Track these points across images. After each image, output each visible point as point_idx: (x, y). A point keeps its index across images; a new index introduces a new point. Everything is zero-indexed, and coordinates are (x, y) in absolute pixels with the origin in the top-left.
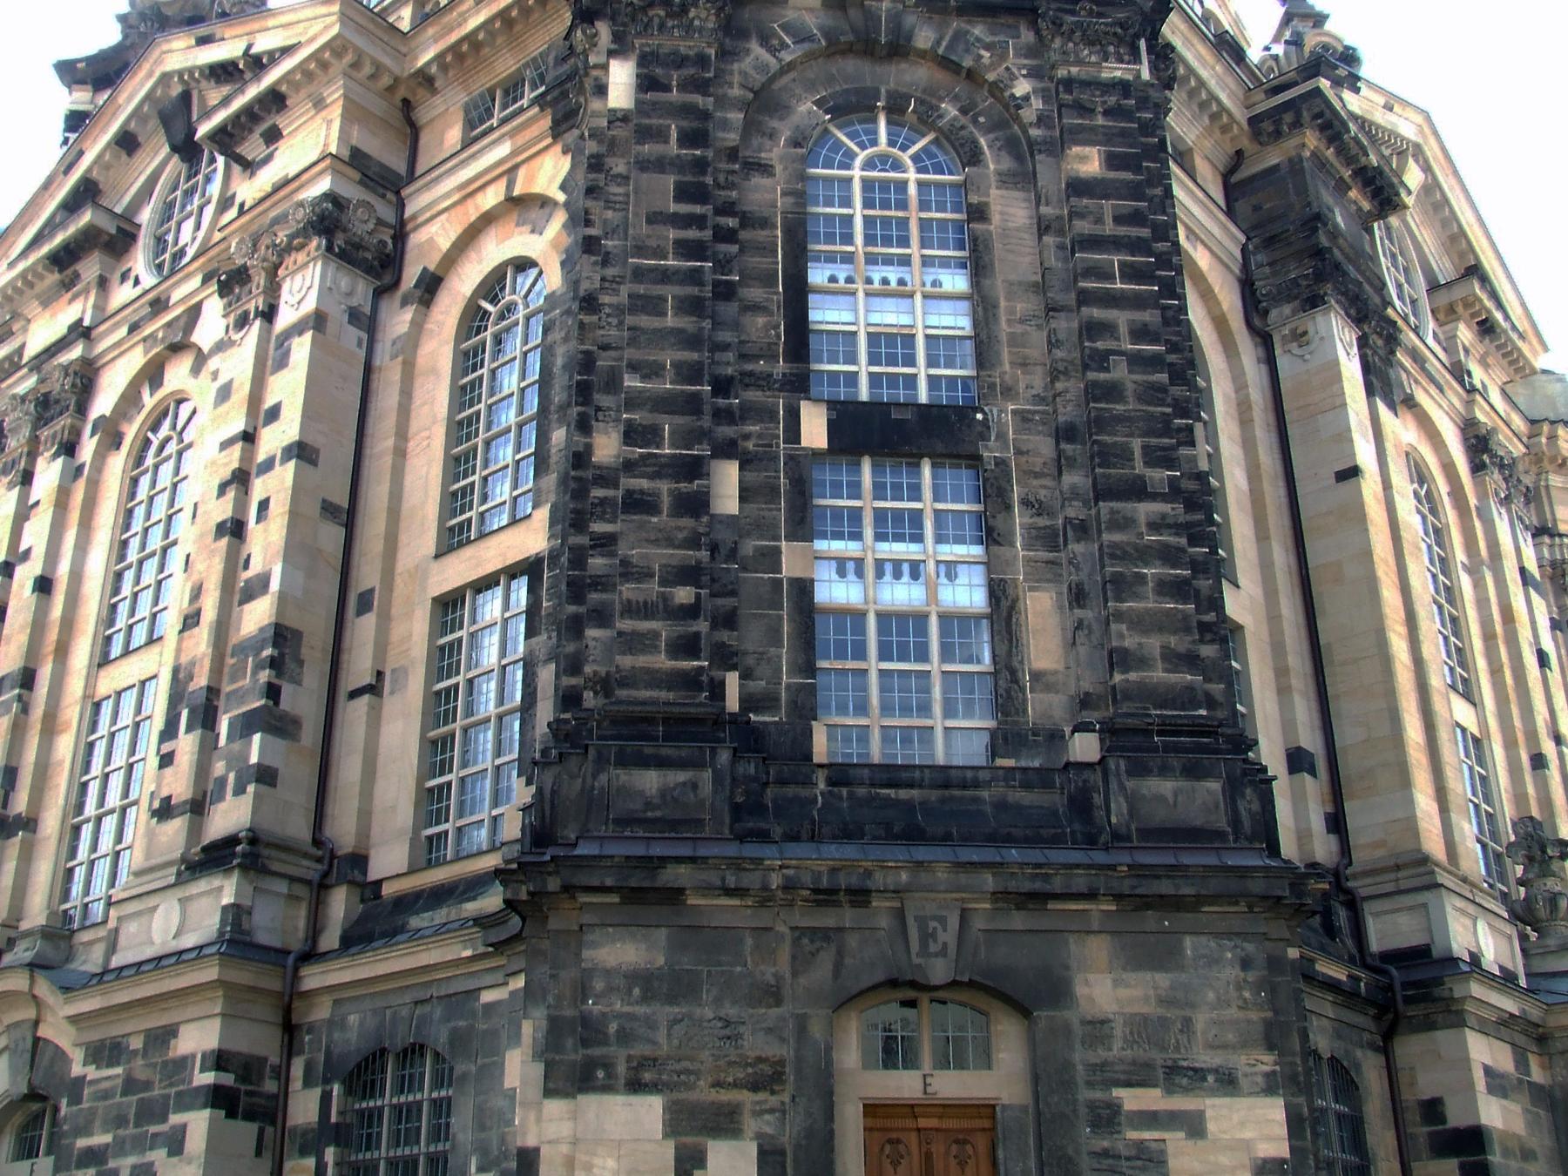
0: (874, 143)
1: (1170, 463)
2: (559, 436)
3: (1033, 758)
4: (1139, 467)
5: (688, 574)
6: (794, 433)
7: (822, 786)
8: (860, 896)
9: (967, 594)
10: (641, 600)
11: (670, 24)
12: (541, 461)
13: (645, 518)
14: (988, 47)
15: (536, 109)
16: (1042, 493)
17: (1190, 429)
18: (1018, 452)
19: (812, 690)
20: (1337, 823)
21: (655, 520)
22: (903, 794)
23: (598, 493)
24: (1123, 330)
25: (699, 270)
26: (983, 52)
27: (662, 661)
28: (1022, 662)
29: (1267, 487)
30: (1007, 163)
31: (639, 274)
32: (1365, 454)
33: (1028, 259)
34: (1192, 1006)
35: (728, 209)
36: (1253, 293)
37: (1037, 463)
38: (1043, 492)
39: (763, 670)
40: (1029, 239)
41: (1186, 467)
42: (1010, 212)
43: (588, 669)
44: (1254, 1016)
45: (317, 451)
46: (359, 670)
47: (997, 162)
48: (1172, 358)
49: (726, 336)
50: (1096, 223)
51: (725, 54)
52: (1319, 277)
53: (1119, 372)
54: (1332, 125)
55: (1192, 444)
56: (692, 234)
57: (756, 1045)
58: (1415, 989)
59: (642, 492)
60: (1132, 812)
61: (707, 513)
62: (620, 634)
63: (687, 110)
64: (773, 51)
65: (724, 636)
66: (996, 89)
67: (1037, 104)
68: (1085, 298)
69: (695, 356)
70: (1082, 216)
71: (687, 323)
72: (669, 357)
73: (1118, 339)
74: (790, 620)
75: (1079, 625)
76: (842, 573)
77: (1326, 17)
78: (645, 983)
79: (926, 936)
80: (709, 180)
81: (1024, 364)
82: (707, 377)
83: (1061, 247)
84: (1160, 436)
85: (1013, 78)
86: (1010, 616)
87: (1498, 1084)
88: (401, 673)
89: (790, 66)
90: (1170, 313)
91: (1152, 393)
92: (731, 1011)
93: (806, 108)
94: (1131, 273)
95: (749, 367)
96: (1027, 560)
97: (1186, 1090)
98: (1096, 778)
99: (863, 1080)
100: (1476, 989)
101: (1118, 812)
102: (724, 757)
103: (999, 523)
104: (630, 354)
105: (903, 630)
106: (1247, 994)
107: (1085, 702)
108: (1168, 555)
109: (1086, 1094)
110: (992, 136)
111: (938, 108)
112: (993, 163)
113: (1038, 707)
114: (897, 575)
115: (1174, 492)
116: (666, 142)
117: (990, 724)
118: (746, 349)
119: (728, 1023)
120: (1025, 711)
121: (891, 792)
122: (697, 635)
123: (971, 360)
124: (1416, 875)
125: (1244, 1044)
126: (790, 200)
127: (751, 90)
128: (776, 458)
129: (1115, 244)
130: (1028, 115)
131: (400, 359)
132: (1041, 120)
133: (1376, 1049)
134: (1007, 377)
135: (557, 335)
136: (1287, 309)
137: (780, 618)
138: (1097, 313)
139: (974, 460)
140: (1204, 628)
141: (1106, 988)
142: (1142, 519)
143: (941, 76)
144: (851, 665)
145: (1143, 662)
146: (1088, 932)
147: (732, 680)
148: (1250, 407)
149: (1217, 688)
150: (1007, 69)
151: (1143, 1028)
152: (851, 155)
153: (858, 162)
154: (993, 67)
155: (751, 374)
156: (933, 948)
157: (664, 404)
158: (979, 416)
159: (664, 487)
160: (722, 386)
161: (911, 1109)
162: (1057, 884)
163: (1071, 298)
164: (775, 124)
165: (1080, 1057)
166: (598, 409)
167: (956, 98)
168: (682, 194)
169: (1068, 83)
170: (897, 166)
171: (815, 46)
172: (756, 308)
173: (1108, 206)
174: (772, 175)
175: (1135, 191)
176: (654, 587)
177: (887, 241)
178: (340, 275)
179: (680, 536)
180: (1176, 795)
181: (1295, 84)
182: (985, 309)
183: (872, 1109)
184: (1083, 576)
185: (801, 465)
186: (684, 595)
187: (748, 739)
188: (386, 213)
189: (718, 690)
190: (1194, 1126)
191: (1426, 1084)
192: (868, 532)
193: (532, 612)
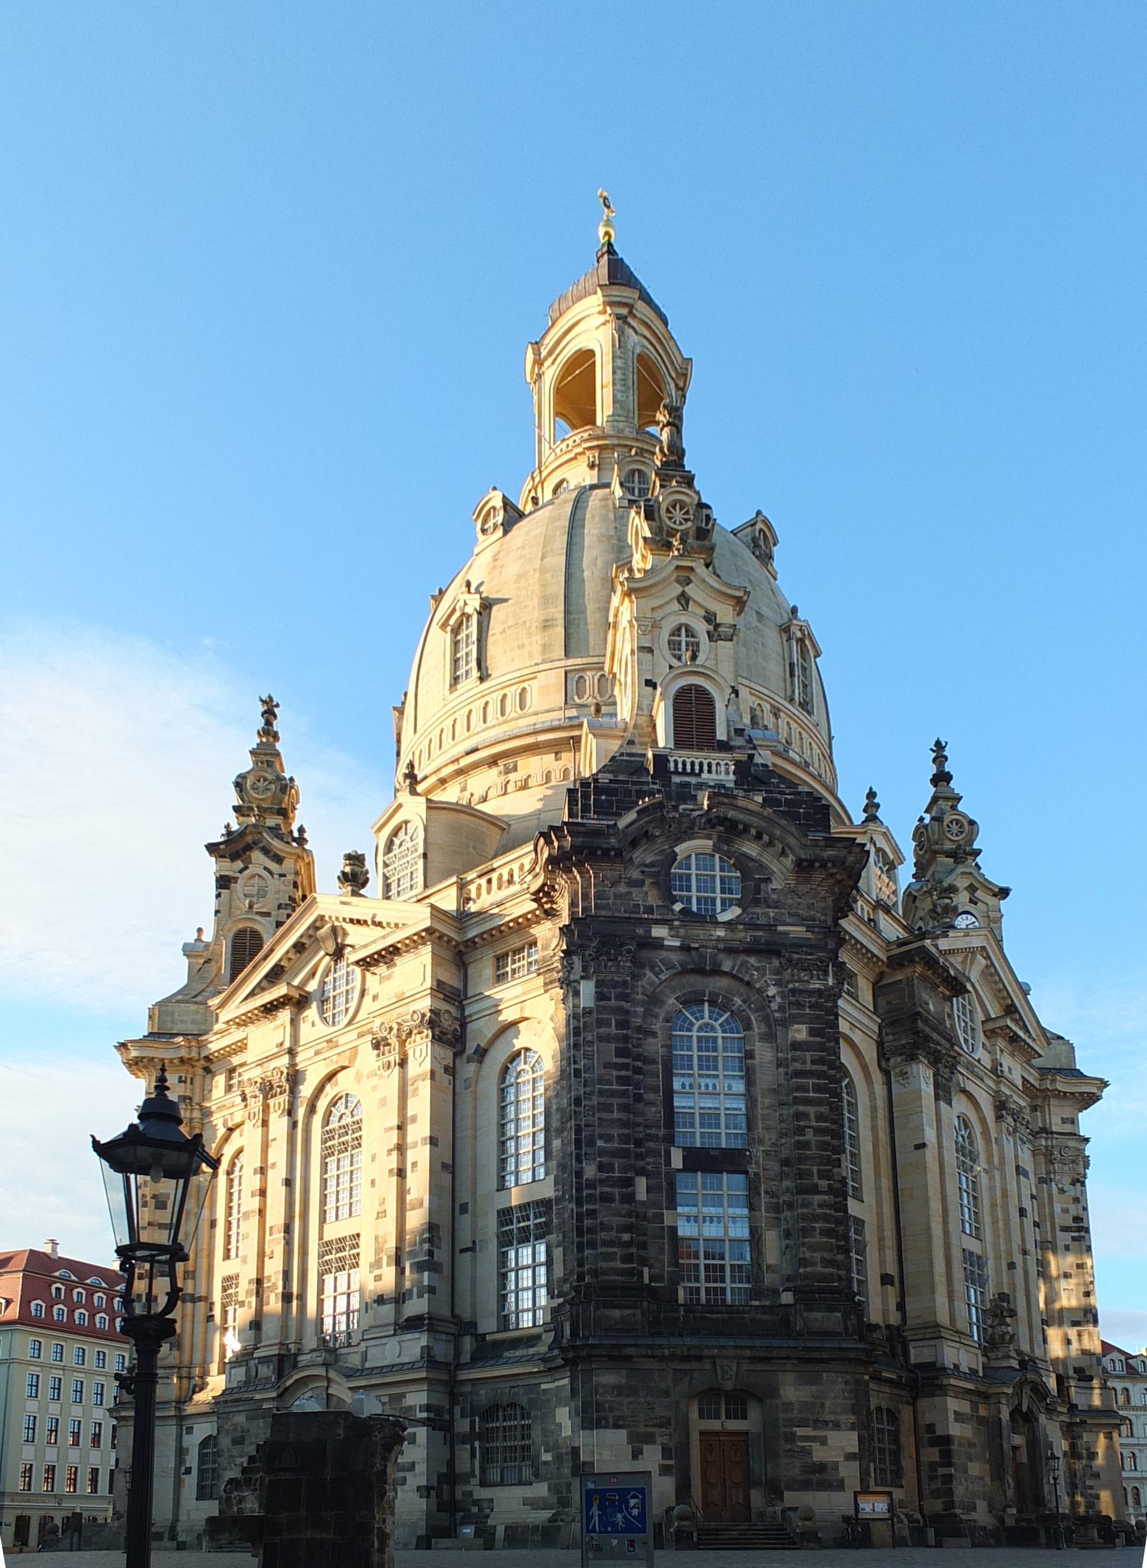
0: (702, 1017)
2: (556, 1143)
4: (816, 1180)
8: (699, 1358)
9: (741, 1231)
16: (774, 1189)
17: (839, 1160)
18: (764, 1169)
22: (714, 1316)
23: (590, 1192)
24: (812, 1116)
27: (619, 1265)
30: (764, 1029)
31: (601, 1093)
33: (770, 1078)
35: (638, 1058)
40: (773, 1067)
41: (836, 1178)
42: (764, 1053)
49: (639, 1120)
51: (635, 977)
52: (915, 1046)
53: (810, 1135)
55: (840, 1166)
56: (623, 1073)
57: (660, 1412)
58: (928, 1380)
61: (635, 1201)
63: (619, 1010)
64: (656, 974)
65: (642, 1252)
67: (778, 999)
69: (627, 1131)
71: (623, 1116)
75: (787, 1247)
79: (724, 1372)
80: (630, 1046)
83: (786, 1074)
85: (768, 986)
87: (960, 1417)
89: (665, 981)
91: (823, 1146)
94: (817, 1089)
99: (698, 1425)
101: (799, 1325)
102: (645, 1304)
107: (789, 1278)
108: (825, 1218)
109: (783, 1429)
112: (757, 1028)
113: (770, 1279)
114: (711, 1222)
115: (830, 1190)
123: (744, 1125)
126: (665, 1049)
128: (660, 1173)
130: (774, 1006)
132: (781, 1008)
136: (899, 1059)
138: (801, 1108)
139: (746, 1172)
141: (792, 1391)
142: (816, 1203)
143: (734, 983)
144: (693, 1261)
145: (813, 1264)
147: (646, 1270)
149: (843, 1273)
152: (692, 1024)
153: (695, 1028)
154: (759, 980)
155: (649, 1135)
157: (615, 1154)
159: (616, 1190)
160: (638, 1143)
161: (716, 1433)
162: (775, 1354)
164: (657, 1010)
165: (781, 1416)
167: (741, 995)
170: (713, 1029)
172: (652, 1103)
173: (808, 1054)
175: (821, 1047)
177: (708, 1069)
186: (626, 1237)
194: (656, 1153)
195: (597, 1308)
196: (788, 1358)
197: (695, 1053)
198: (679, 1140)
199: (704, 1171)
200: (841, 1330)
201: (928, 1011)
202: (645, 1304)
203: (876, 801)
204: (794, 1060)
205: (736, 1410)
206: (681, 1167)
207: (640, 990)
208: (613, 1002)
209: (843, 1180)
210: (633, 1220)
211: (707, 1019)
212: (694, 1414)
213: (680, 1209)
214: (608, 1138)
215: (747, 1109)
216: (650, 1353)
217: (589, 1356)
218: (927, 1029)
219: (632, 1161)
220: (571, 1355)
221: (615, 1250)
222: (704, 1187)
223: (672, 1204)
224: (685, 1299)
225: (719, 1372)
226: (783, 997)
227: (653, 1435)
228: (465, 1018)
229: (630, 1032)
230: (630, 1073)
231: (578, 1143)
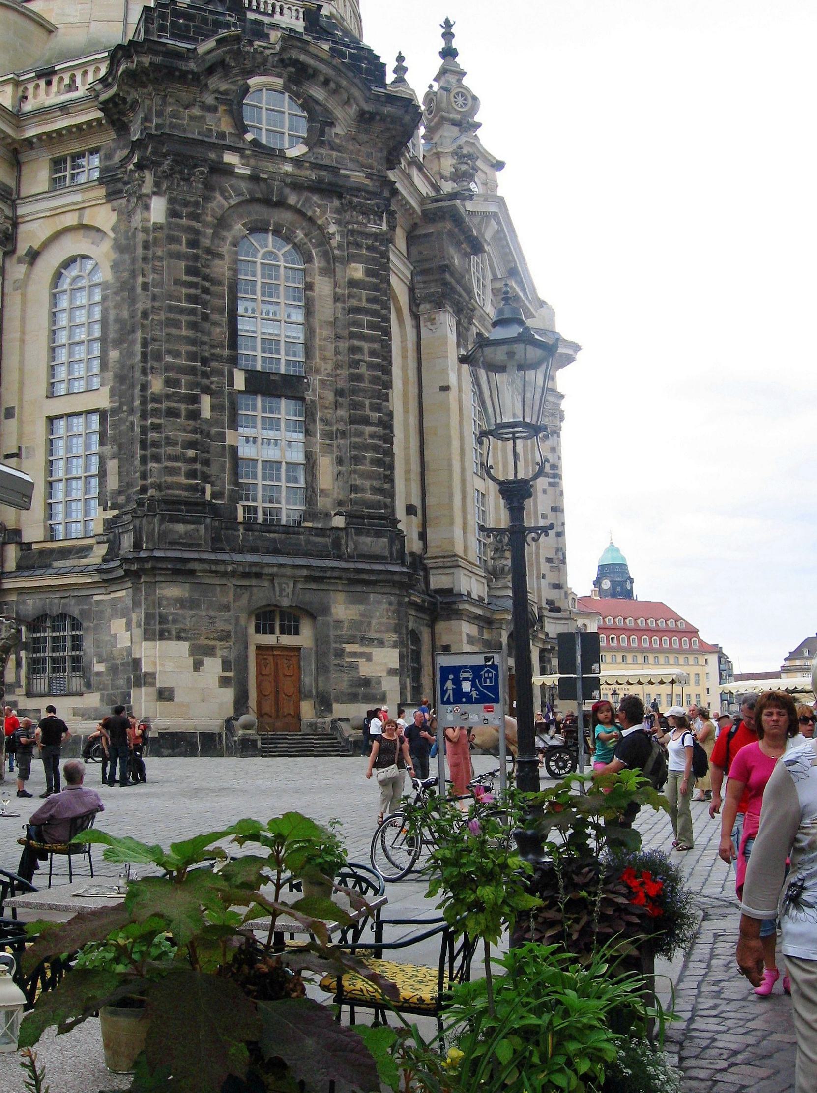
2: (114, 355)
4: (368, 412)
6: (231, 383)
7: (242, 530)
8: (258, 575)
9: (297, 456)
11: (182, 183)
12: (104, 366)
14: (319, 206)
15: (97, 183)
17: (387, 394)
18: (320, 398)
20: (423, 536)
22: (272, 535)
23: (156, 406)
24: (366, 351)
27: (183, 480)
30: (323, 264)
31: (171, 309)
32: (453, 380)
34: (371, 617)
35: (206, 278)
36: (414, 294)
38: (329, 416)
39: (218, 482)
40: (330, 301)
41: (384, 411)
42: (323, 287)
44: (392, 622)
47: (319, 263)
48: (384, 363)
49: (206, 338)
51: (207, 199)
52: (444, 295)
53: (363, 369)
54: (457, 219)
56: (192, 291)
57: (220, 625)
58: (443, 606)
59: (174, 408)
60: (356, 548)
63: (190, 230)
64: (226, 198)
65: (205, 469)
66: (321, 228)
67: (338, 238)
68: (352, 335)
71: (190, 333)
74: (230, 463)
75: (339, 473)
76: (247, 441)
77: (464, 74)
78: (181, 602)
79: (282, 590)
80: (199, 265)
81: (324, 359)
82: (199, 359)
83: (344, 309)
85: (329, 223)
86: (313, 467)
90: (384, 343)
91: (375, 380)
92: (212, 614)
93: (238, 228)
94: (372, 326)
95: (213, 351)
96: (321, 444)
97: (367, 646)
98: (343, 534)
100: (467, 607)
101: (351, 546)
102: (208, 521)
103: (311, 427)
104: (170, 346)
105: (272, 466)
107: (340, 503)
108: (375, 448)
112: (318, 262)
113: (322, 503)
115: (381, 423)
116: (181, 245)
117: (303, 508)
118: (215, 343)
119: (211, 618)
124: (451, 562)
125: (388, 631)
126: (231, 273)
129: (367, 311)
130: (334, 243)
131: (19, 291)
132: (339, 247)
133: (428, 626)
135: (110, 304)
136: (428, 306)
138: (356, 342)
140: (386, 476)
141: (342, 609)
142: (367, 433)
145: (363, 490)
147: (208, 487)
148: (407, 351)
151: (354, 624)
153: (260, 255)
154: (320, 218)
156: (284, 594)
159: (183, 407)
160: (205, 361)
161: (271, 648)
162: (328, 574)
163: (345, 333)
164: (225, 234)
165: (332, 633)
166: (152, 368)
167: (303, 229)
168: (190, 271)
169: (352, 232)
172: (215, 324)
173: (364, 292)
175: (376, 288)
176: (179, 449)
179: (190, 428)
183: (259, 648)
184: (342, 453)
185: (233, 396)
186: (191, 453)
187: (215, 510)
188: (8, 212)
190: (369, 657)
191: (445, 640)
192: (259, 425)
193: (103, 435)
194: (221, 374)
195: (162, 521)
196: (340, 578)
197: (259, 280)
198: (242, 363)
199: (264, 394)
200: (387, 554)
201: (453, 265)
202: (208, 521)
203: (404, 64)
204: (350, 296)
205: (289, 627)
206: (244, 389)
208: (184, 221)
209: (390, 415)
210: (198, 436)
211: (270, 248)
212: (252, 630)
213: (241, 430)
214: (176, 354)
215: (306, 339)
216: (214, 568)
217: (154, 568)
218: (453, 281)
219: (199, 379)
220: (135, 567)
221: (179, 464)
222: (264, 411)
223: (234, 424)
224: (244, 517)
225: (277, 589)
226: (342, 237)
227: (213, 648)
229: (200, 252)
230: (199, 292)
231: (144, 355)
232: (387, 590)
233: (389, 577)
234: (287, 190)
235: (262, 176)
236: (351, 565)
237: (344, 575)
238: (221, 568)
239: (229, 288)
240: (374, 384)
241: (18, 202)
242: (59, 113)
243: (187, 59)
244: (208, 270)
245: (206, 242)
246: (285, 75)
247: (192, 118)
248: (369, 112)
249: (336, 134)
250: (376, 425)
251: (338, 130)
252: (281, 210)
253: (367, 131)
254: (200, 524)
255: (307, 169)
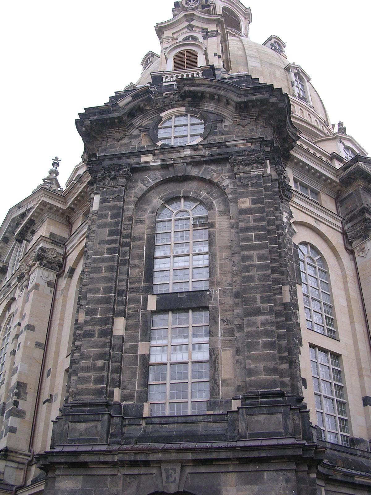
1: (269, 301)
3: (220, 410)
4: (259, 304)
5: (101, 356)
7: (144, 425)
8: (146, 464)
9: (204, 355)
10: (86, 366)
13: (90, 339)
14: (215, 171)
18: (221, 304)
19: (147, 393)
21: (93, 339)
24: (255, 257)
25: (114, 257)
26: (213, 173)
27: (91, 386)
28: (218, 377)
29: (353, 304)
30: (222, 207)
31: (95, 261)
35: (128, 236)
36: (347, 237)
37: (227, 307)
38: (229, 316)
39: (130, 387)
42: (222, 223)
43: (71, 390)
45: (34, 327)
46: (45, 396)
47: (219, 208)
50: (247, 223)
53: (254, 273)
56: (113, 245)
59: (90, 330)
62: (79, 378)
63: (114, 207)
66: (217, 185)
67: (231, 187)
68: (243, 248)
70: (242, 221)
71: (108, 274)
72: (102, 286)
73: (253, 261)
81: (224, 274)
84: (267, 292)
85: (223, 180)
86: (215, 361)
88: (57, 394)
93: (156, 201)
94: (258, 238)
101: (242, 426)
104: (90, 286)
106: (287, 492)
108: (268, 334)
110: (217, 200)
111: (200, 193)
113: (224, 391)
117: (207, 399)
120: (219, 394)
121: (167, 426)
122: (103, 376)
126: (150, 230)
127: (137, 198)
128: (139, 315)
129: (254, 228)
134: (218, 279)
136: (358, 241)
137: (136, 368)
138: (246, 253)
140: (281, 358)
142: (259, 322)
145: (257, 373)
146: (228, 472)
149: (287, 380)
150: (222, 177)
154: (217, 177)
156: (171, 480)
158: (208, 293)
159: (97, 328)
160: (120, 293)
162: (214, 456)
164: (146, 207)
167: (206, 189)
169: (240, 178)
171: (158, 181)
172: (136, 267)
173: (251, 216)
174: (144, 223)
178: (44, 271)
179: (101, 344)
180: (264, 420)
181: (352, 165)
182: (212, 257)
186: (100, 363)
188: (61, 251)
189: (112, 394)
194: (137, 301)
206: (155, 308)
207: (133, 195)
208: (111, 203)
213: (153, 343)
214: (97, 291)
216: (102, 459)
221: (89, 374)
225: (164, 475)
228: (66, 253)
232: (284, 466)
233: (281, 453)
234: (189, 168)
235: (168, 163)
236: (241, 444)
237: (230, 455)
238: (108, 458)
239: (148, 240)
240: (263, 281)
241: (66, 244)
242: (79, 184)
243: (113, 112)
244: (130, 231)
245: (128, 214)
246: (186, 104)
247: (121, 145)
248: (242, 102)
249: (226, 126)
250: (267, 314)
251: (227, 123)
252: (190, 182)
253: (246, 117)
254: (98, 421)
255: (201, 150)
